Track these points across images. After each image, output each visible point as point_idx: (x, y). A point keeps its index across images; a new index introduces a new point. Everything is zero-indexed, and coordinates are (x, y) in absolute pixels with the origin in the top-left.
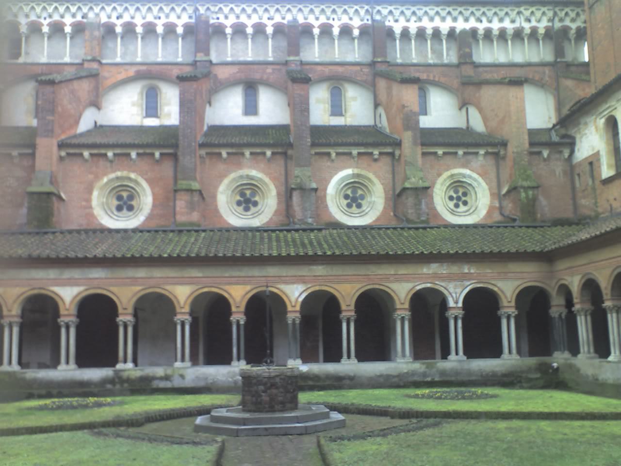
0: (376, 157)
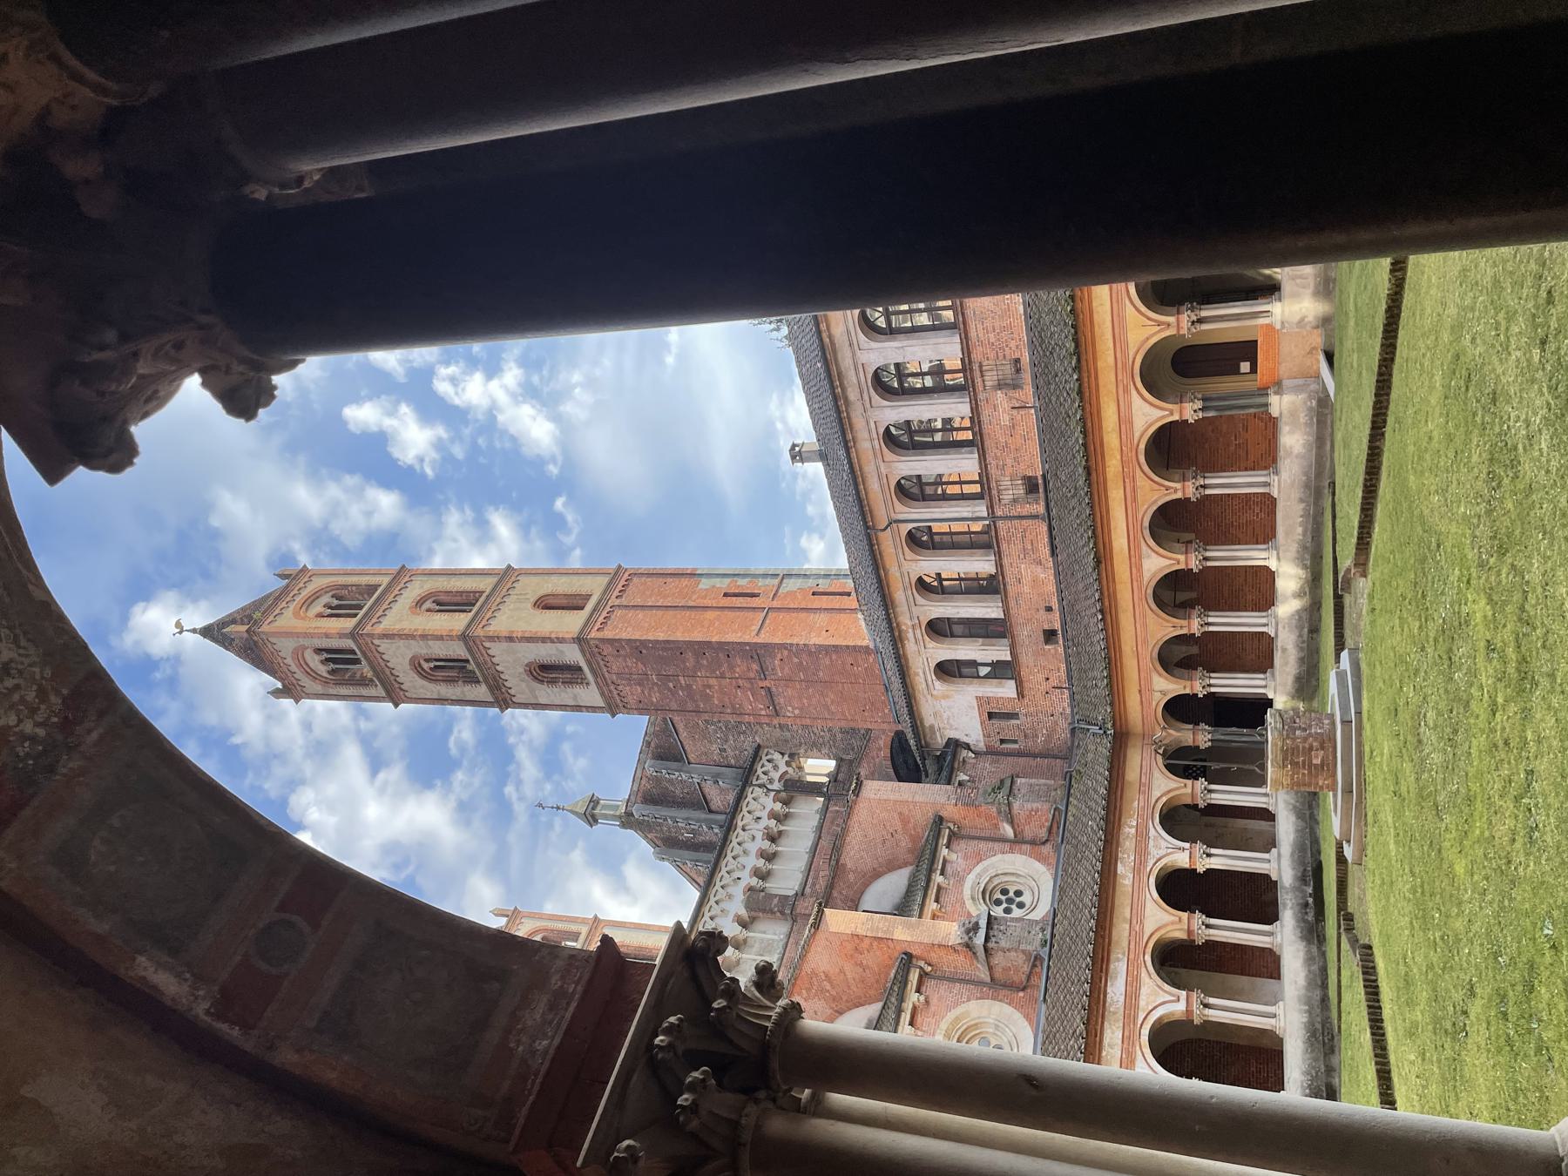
0: (922, 998)
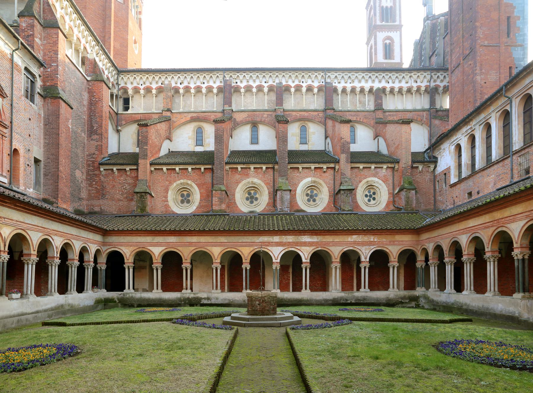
0: (325, 170)
